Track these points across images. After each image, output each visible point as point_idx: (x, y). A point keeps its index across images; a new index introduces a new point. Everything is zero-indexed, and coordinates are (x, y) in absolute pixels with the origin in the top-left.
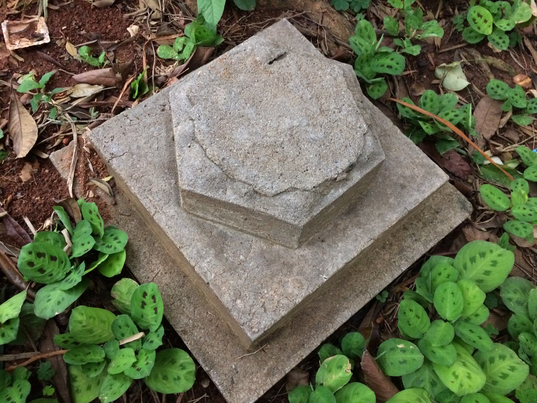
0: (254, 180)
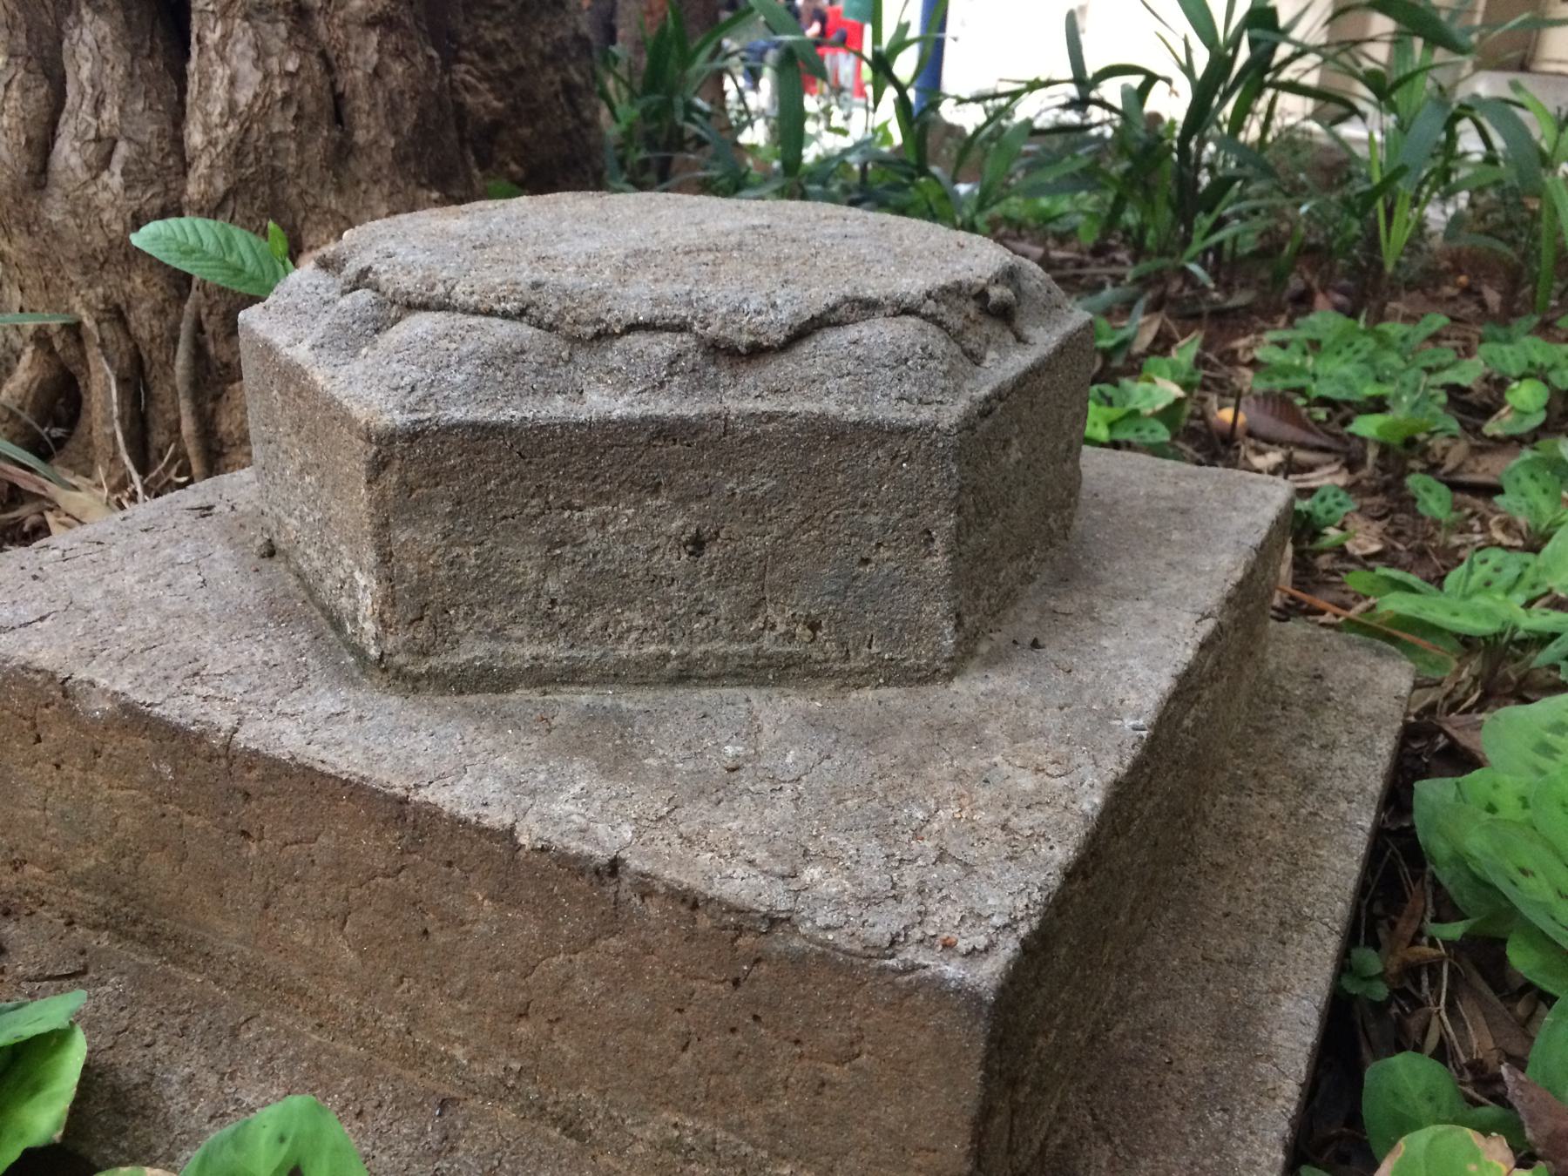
0: (690, 304)
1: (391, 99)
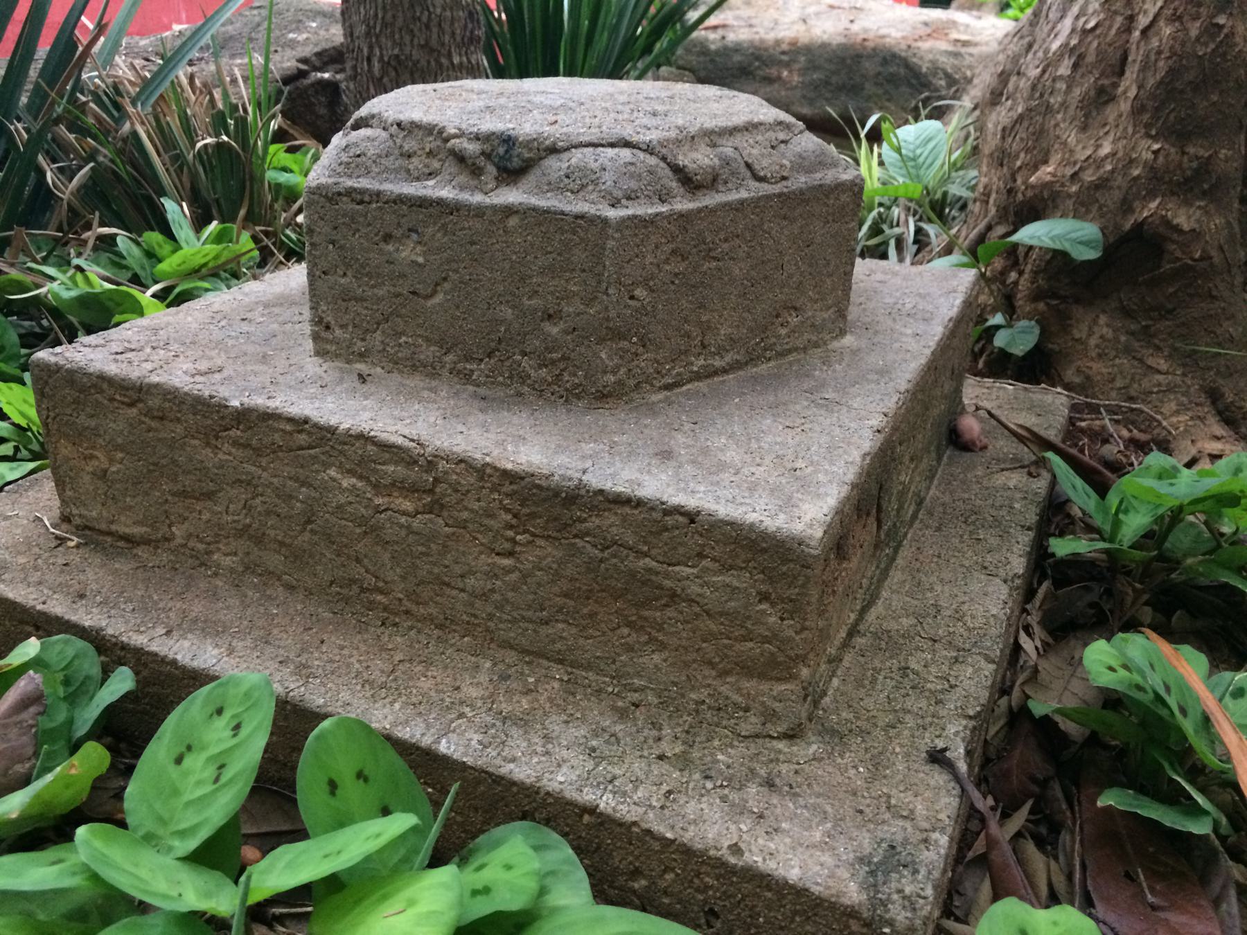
1: (1148, 56)
